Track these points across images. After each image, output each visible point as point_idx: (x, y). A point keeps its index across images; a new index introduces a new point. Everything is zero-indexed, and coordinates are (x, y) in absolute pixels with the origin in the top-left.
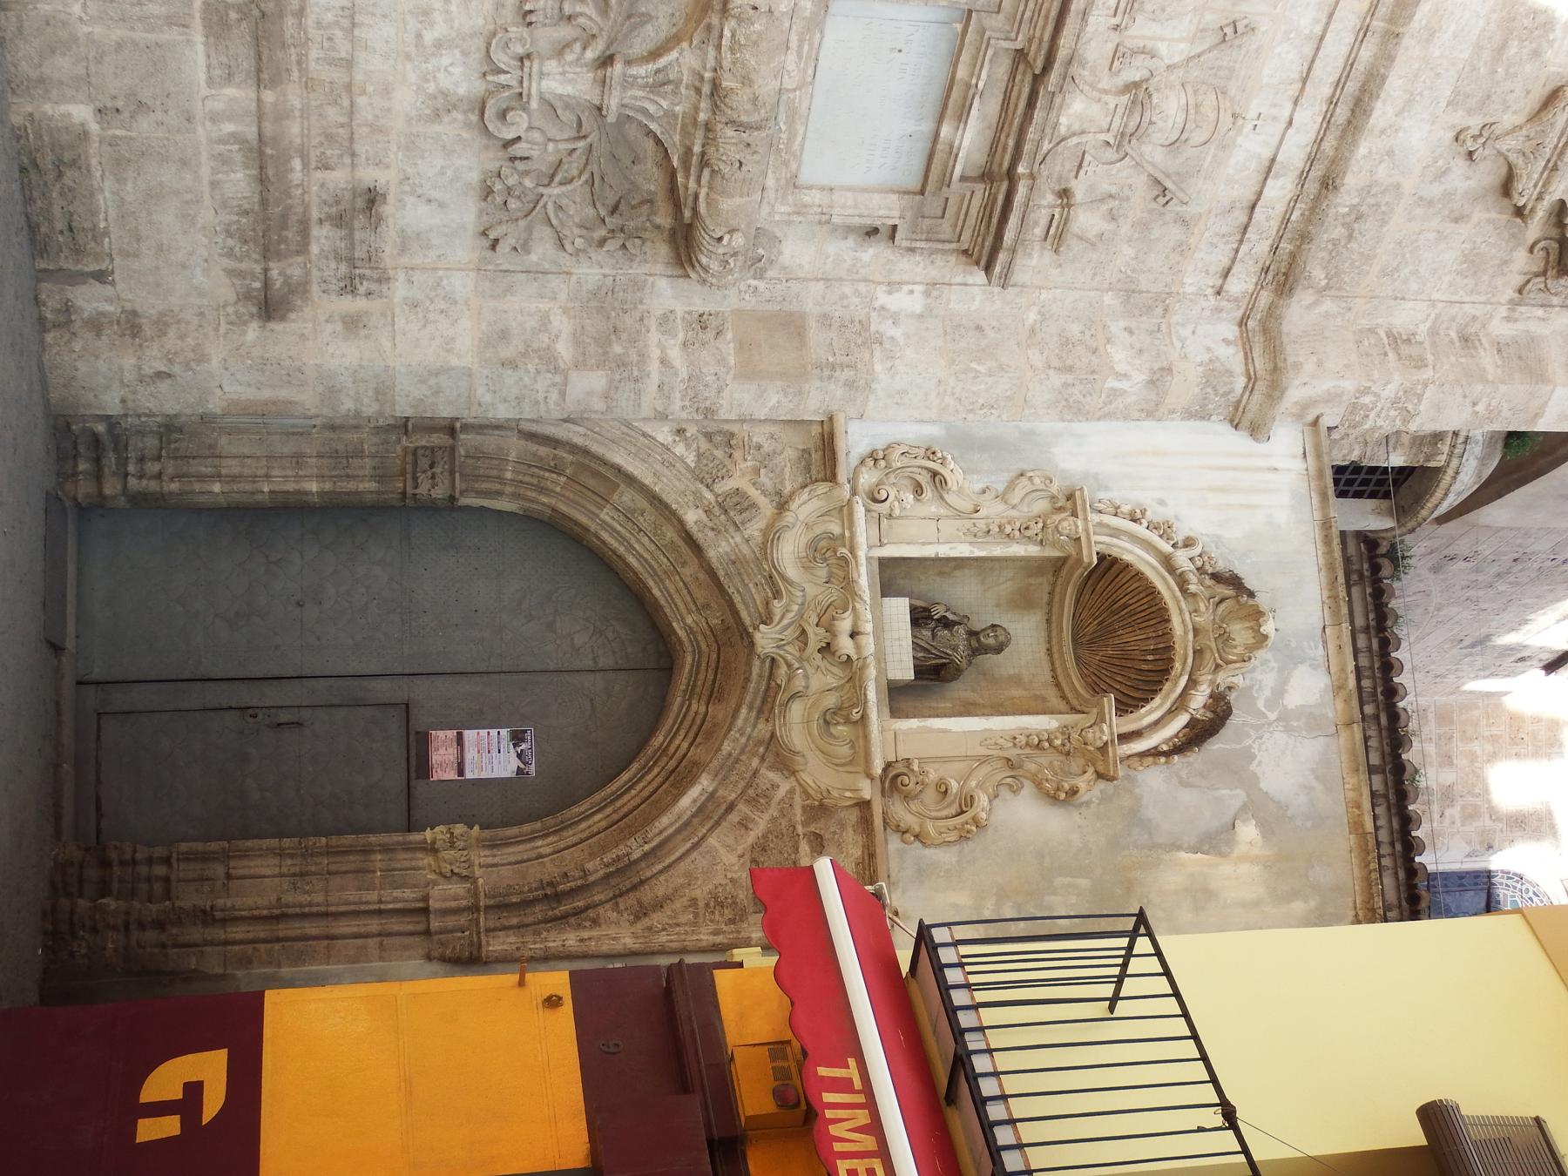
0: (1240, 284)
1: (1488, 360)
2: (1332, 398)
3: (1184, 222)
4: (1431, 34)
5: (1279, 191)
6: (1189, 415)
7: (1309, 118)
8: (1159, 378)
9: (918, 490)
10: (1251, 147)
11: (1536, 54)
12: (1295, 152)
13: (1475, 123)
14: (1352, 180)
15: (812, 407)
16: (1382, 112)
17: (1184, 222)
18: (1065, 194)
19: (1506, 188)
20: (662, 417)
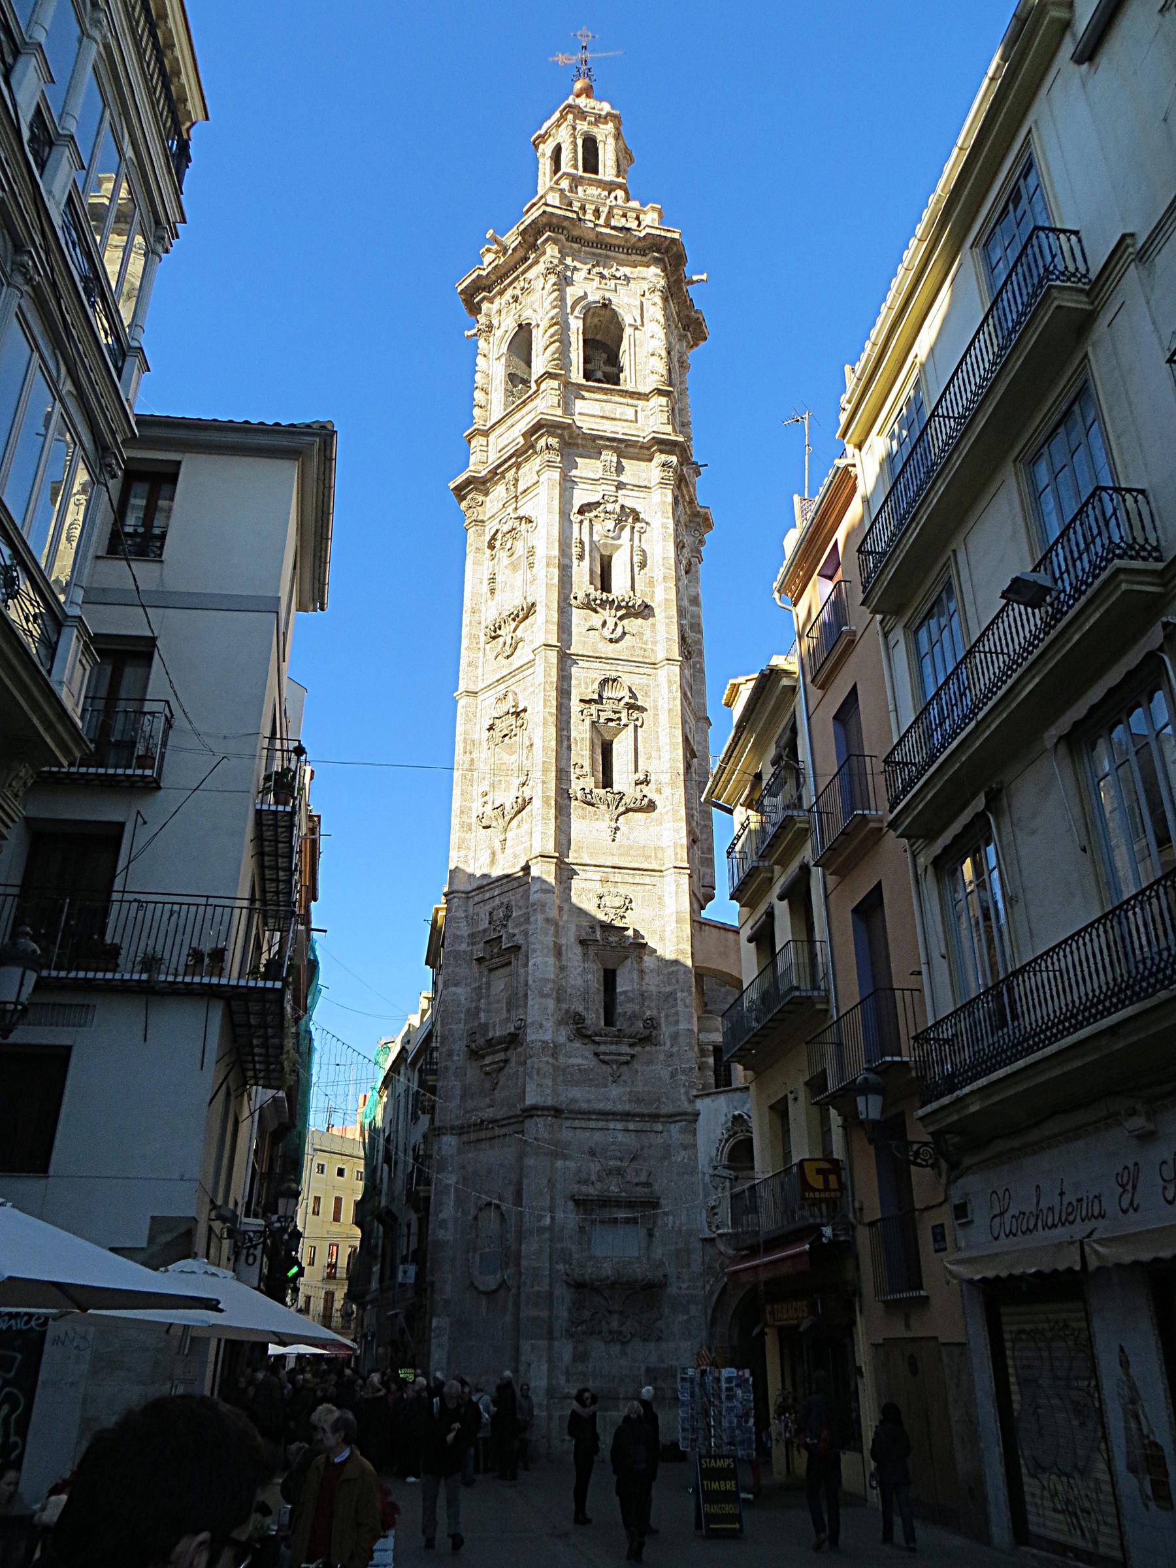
0: (659, 1127)
1: (675, 1049)
2: (687, 1093)
3: (642, 1148)
4: (588, 1101)
5: (631, 1126)
6: (695, 1134)
7: (612, 1125)
8: (685, 1147)
9: (716, 1214)
10: (620, 1137)
11: (592, 1070)
12: (619, 1126)
13: (610, 1078)
14: (627, 1107)
15: (699, 1245)
16: (609, 1107)
17: (642, 1148)
18: (637, 1184)
19: (627, 1063)
20: (704, 1287)
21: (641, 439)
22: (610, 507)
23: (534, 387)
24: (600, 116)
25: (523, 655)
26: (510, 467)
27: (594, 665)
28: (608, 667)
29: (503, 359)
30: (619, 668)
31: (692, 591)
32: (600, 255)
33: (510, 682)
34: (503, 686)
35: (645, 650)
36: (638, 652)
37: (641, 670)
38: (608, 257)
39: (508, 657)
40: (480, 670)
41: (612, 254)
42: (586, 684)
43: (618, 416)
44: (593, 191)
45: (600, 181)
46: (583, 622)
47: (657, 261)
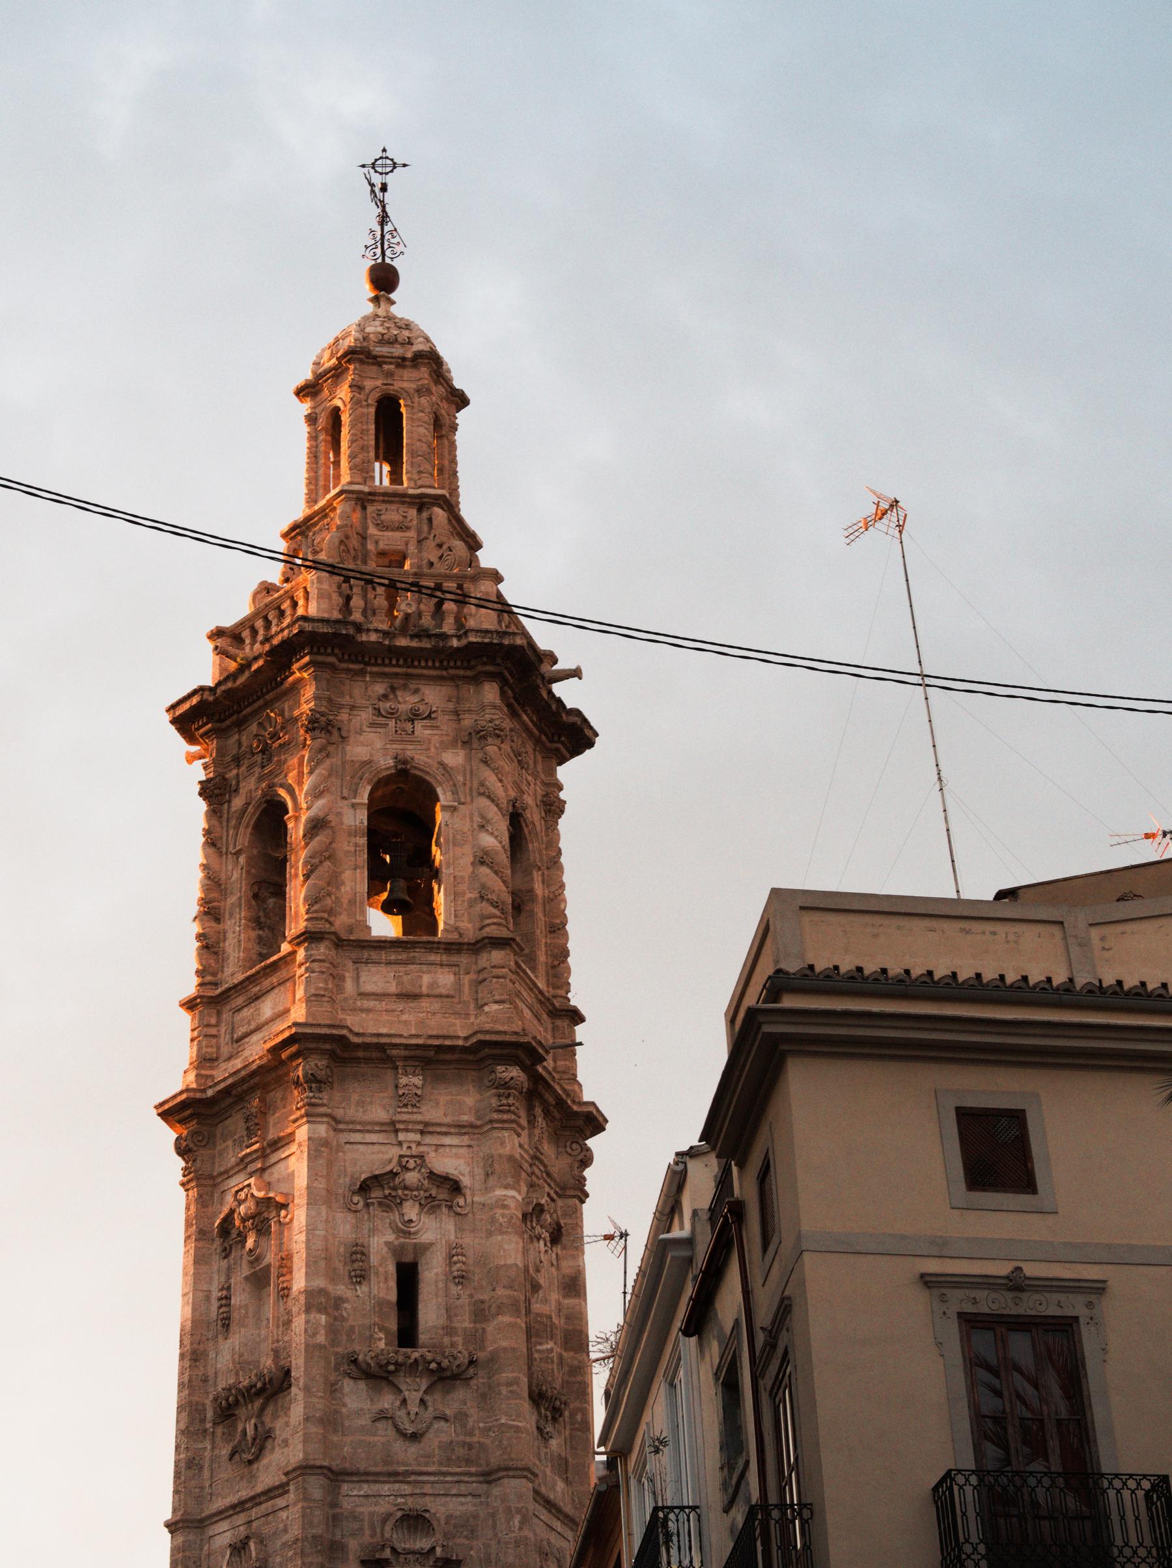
21: (460, 1043)
22: (412, 1178)
23: (285, 948)
24: (404, 359)
25: (269, 1473)
26: (252, 1089)
27: (386, 1489)
28: (406, 1489)
29: (242, 859)
30: (428, 1489)
31: (567, 1266)
32: (396, 675)
33: (254, 1513)
34: (241, 1519)
35: (470, 1446)
36: (461, 1452)
37: (463, 1488)
38: (409, 676)
39: (250, 1462)
40: (206, 1473)
41: (419, 671)
42: (372, 1527)
43: (424, 990)
44: (393, 514)
45: (404, 495)
46: (367, 1405)
47: (491, 676)
